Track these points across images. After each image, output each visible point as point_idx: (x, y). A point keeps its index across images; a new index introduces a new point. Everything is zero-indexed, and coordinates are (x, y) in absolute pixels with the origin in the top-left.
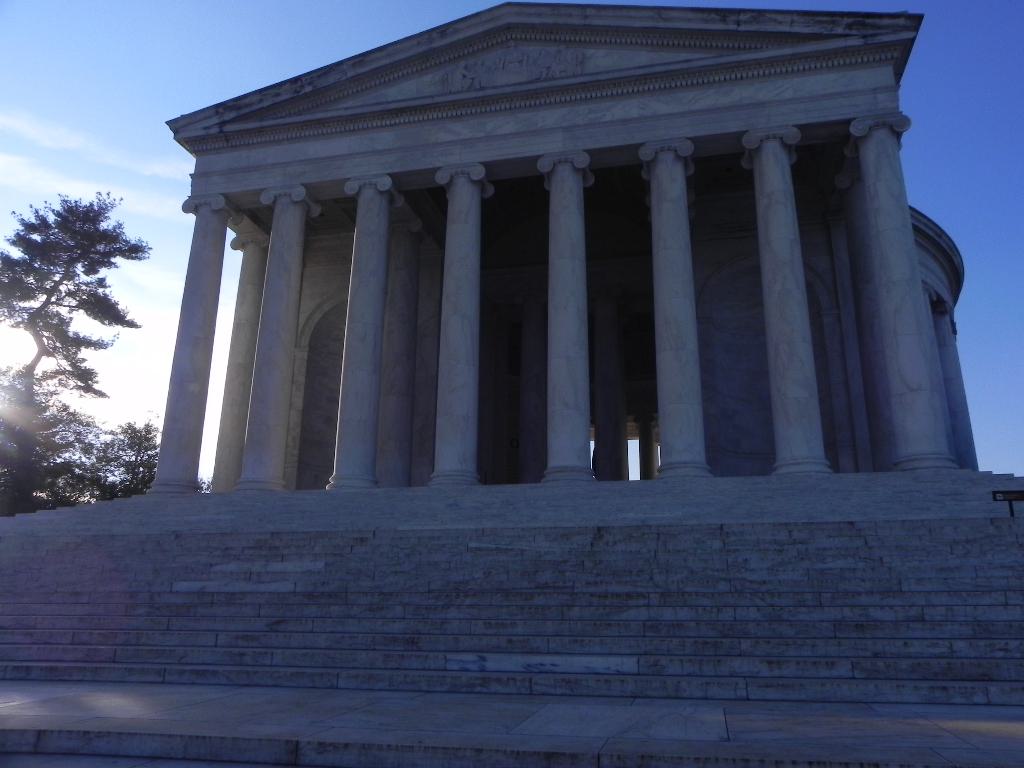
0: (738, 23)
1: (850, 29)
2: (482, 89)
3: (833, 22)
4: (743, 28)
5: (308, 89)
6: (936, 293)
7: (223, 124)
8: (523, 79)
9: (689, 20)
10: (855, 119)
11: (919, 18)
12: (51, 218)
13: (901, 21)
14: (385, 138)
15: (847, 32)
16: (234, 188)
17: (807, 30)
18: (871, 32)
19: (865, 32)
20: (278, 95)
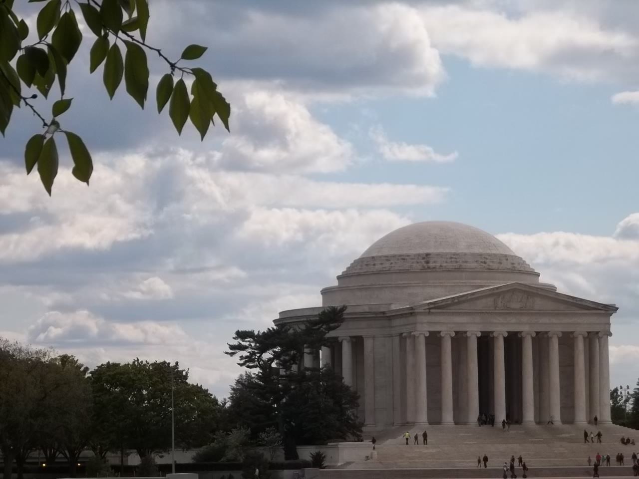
0: (576, 301)
4: (577, 302)
11: (617, 309)
13: (614, 309)
14: (478, 319)
18: (607, 309)
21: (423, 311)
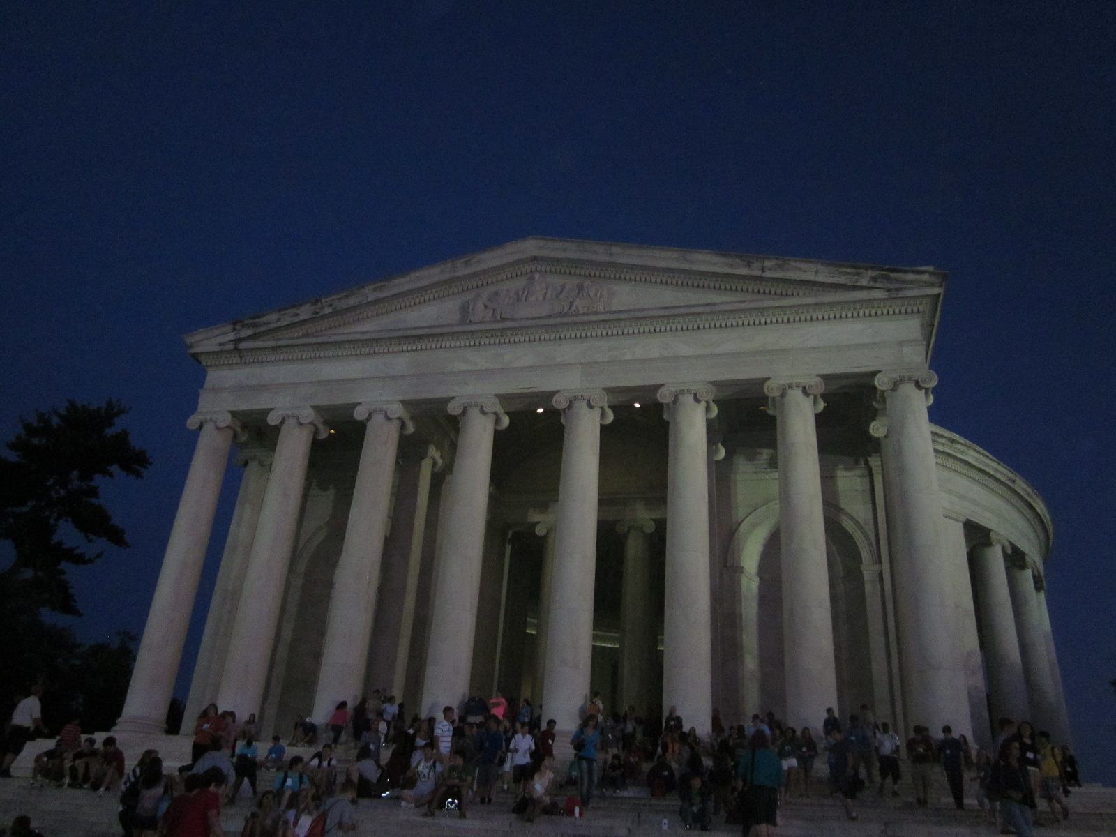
1: (876, 282)
2: (503, 319)
3: (858, 274)
4: (768, 274)
5: (328, 310)
6: (1011, 544)
7: (238, 341)
8: (544, 314)
9: (715, 264)
10: (880, 372)
12: (55, 421)
14: (400, 363)
15: (872, 284)
16: (243, 406)
17: (830, 280)
19: (890, 286)
20: (297, 315)
21: (217, 348)
